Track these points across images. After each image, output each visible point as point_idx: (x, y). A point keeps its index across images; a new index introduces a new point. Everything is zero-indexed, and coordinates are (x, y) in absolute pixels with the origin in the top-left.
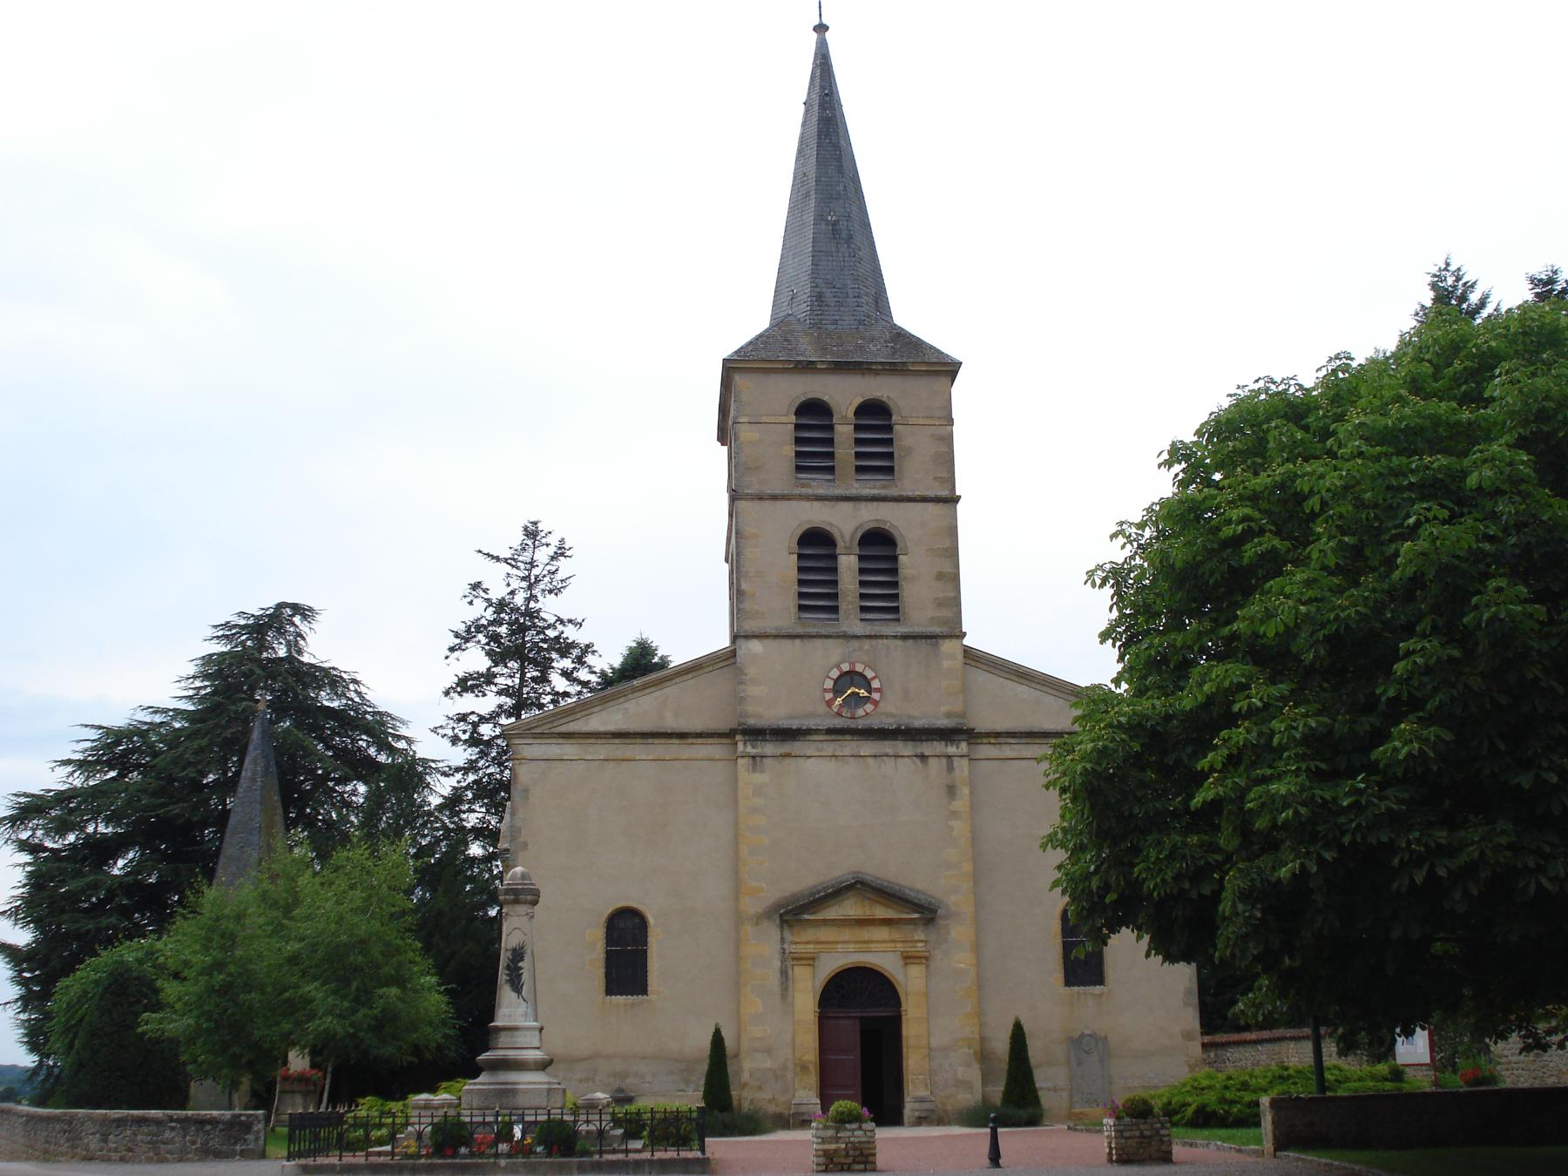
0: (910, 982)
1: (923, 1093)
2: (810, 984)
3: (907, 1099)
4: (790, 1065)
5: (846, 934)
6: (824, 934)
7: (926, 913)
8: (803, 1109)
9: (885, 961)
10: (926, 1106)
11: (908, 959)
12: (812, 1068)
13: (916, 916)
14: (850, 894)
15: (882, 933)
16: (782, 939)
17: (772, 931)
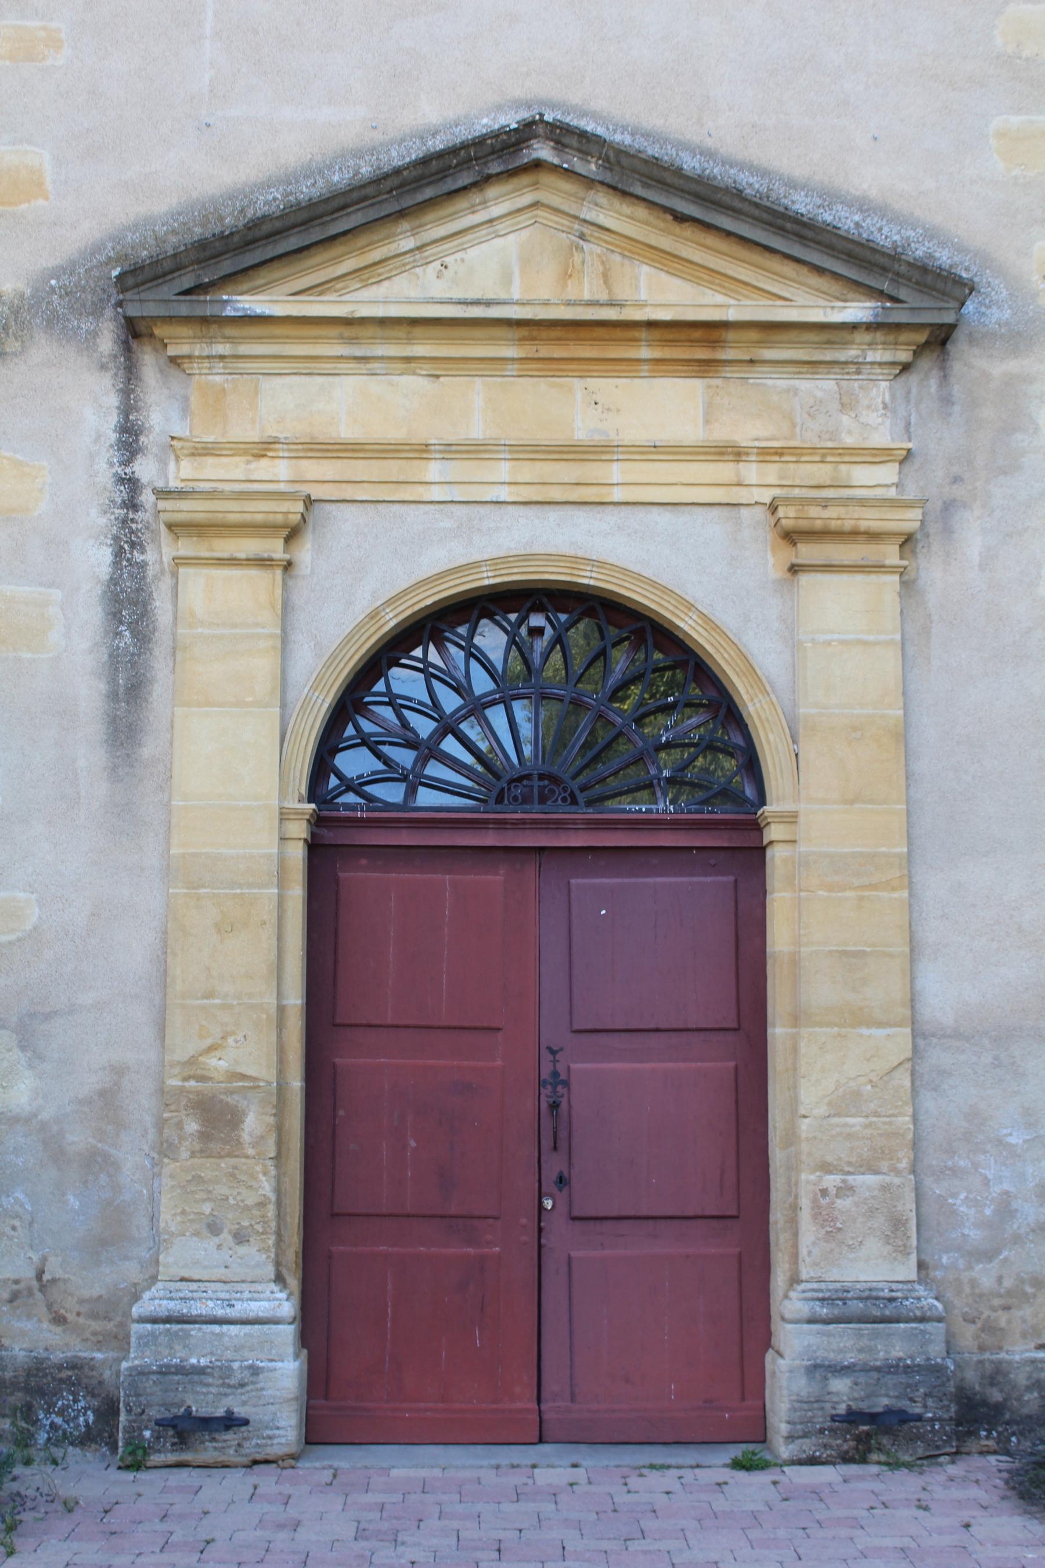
0: (799, 656)
1: (873, 1265)
2: (262, 666)
3: (789, 1304)
4: (141, 1105)
5: (477, 405)
6: (349, 401)
7: (922, 307)
8: (198, 1350)
9: (686, 562)
10: (895, 1345)
11: (803, 539)
12: (255, 1122)
13: (858, 310)
14: (500, 201)
15: (665, 406)
16: (130, 439)
17: (74, 392)
